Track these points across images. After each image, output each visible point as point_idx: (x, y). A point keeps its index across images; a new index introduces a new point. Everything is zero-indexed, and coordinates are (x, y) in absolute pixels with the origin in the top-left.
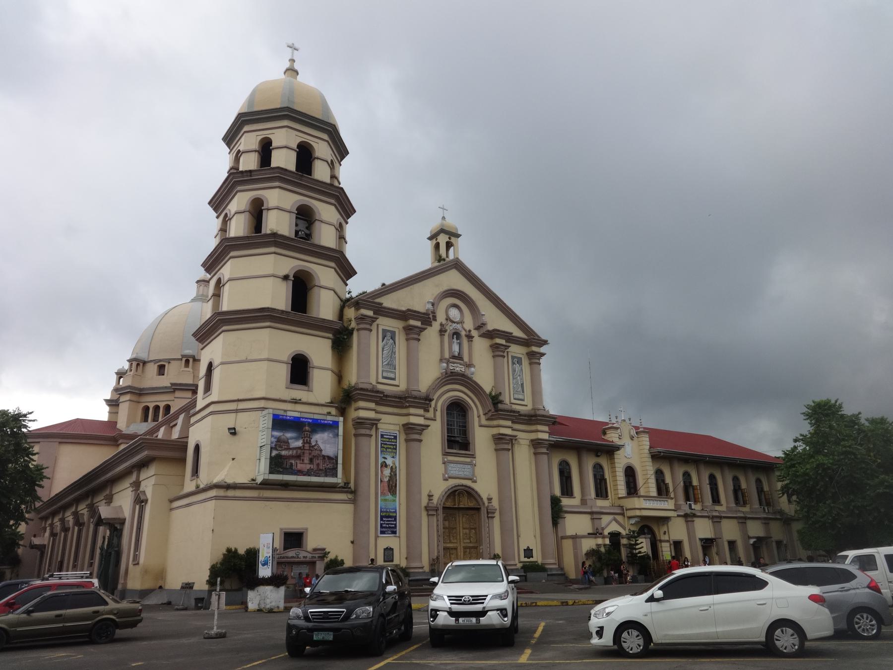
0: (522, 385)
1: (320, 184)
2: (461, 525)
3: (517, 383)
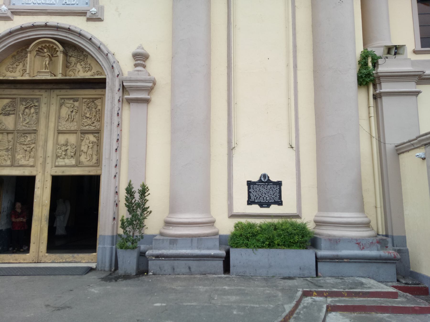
2: (52, 125)
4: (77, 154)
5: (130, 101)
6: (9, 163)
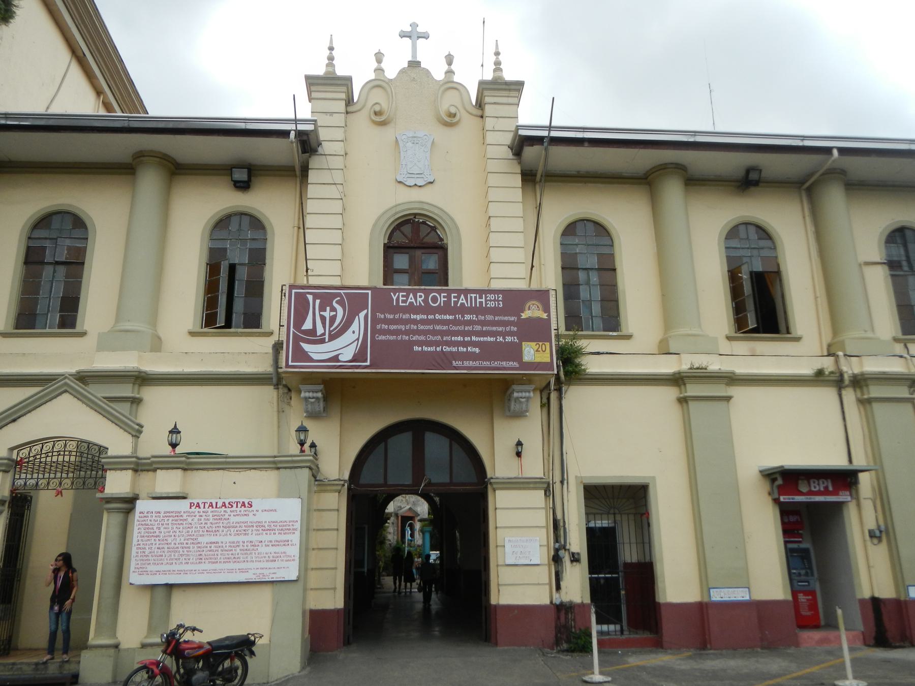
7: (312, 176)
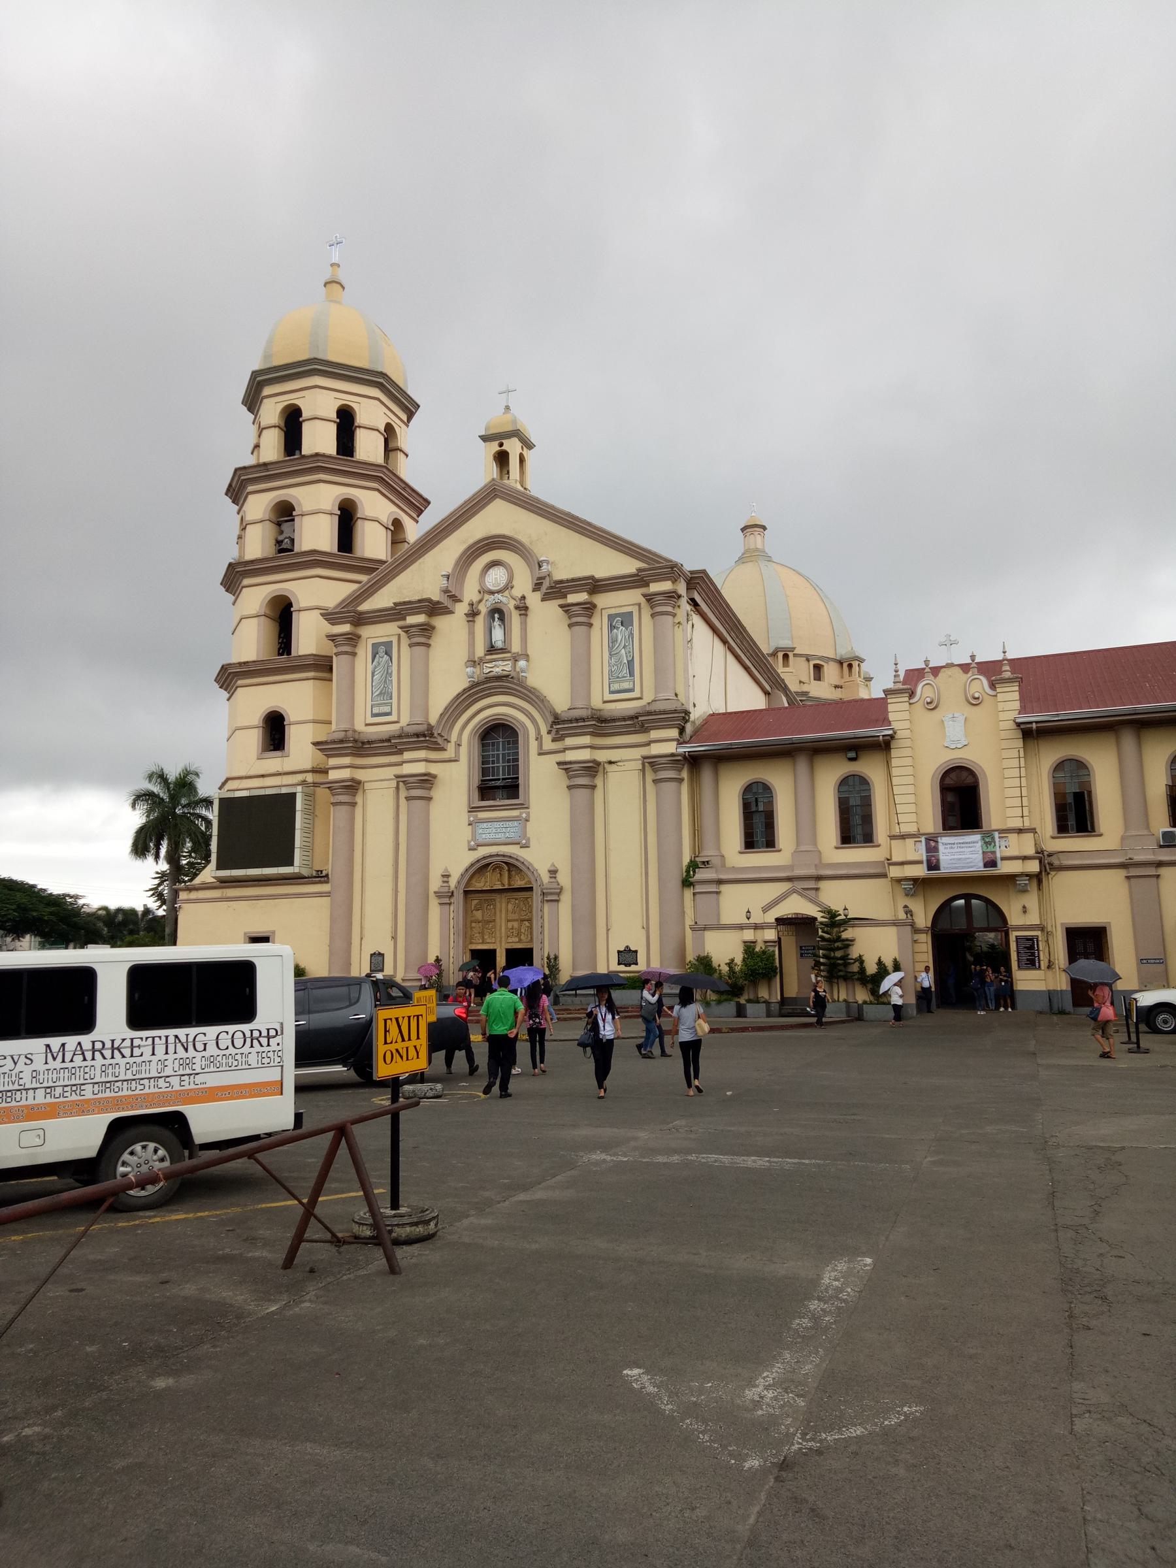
0: (630, 663)
1: (277, 466)
2: (503, 916)
3: (620, 661)
4: (519, 934)
5: (548, 901)
6: (481, 941)
7: (894, 753)
